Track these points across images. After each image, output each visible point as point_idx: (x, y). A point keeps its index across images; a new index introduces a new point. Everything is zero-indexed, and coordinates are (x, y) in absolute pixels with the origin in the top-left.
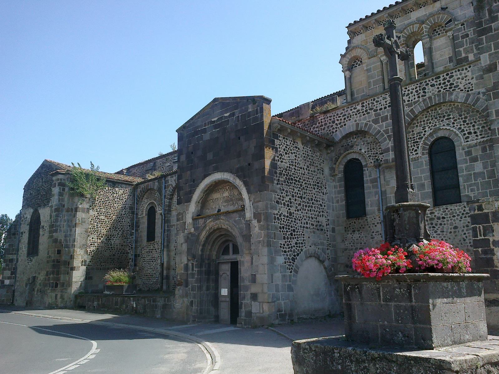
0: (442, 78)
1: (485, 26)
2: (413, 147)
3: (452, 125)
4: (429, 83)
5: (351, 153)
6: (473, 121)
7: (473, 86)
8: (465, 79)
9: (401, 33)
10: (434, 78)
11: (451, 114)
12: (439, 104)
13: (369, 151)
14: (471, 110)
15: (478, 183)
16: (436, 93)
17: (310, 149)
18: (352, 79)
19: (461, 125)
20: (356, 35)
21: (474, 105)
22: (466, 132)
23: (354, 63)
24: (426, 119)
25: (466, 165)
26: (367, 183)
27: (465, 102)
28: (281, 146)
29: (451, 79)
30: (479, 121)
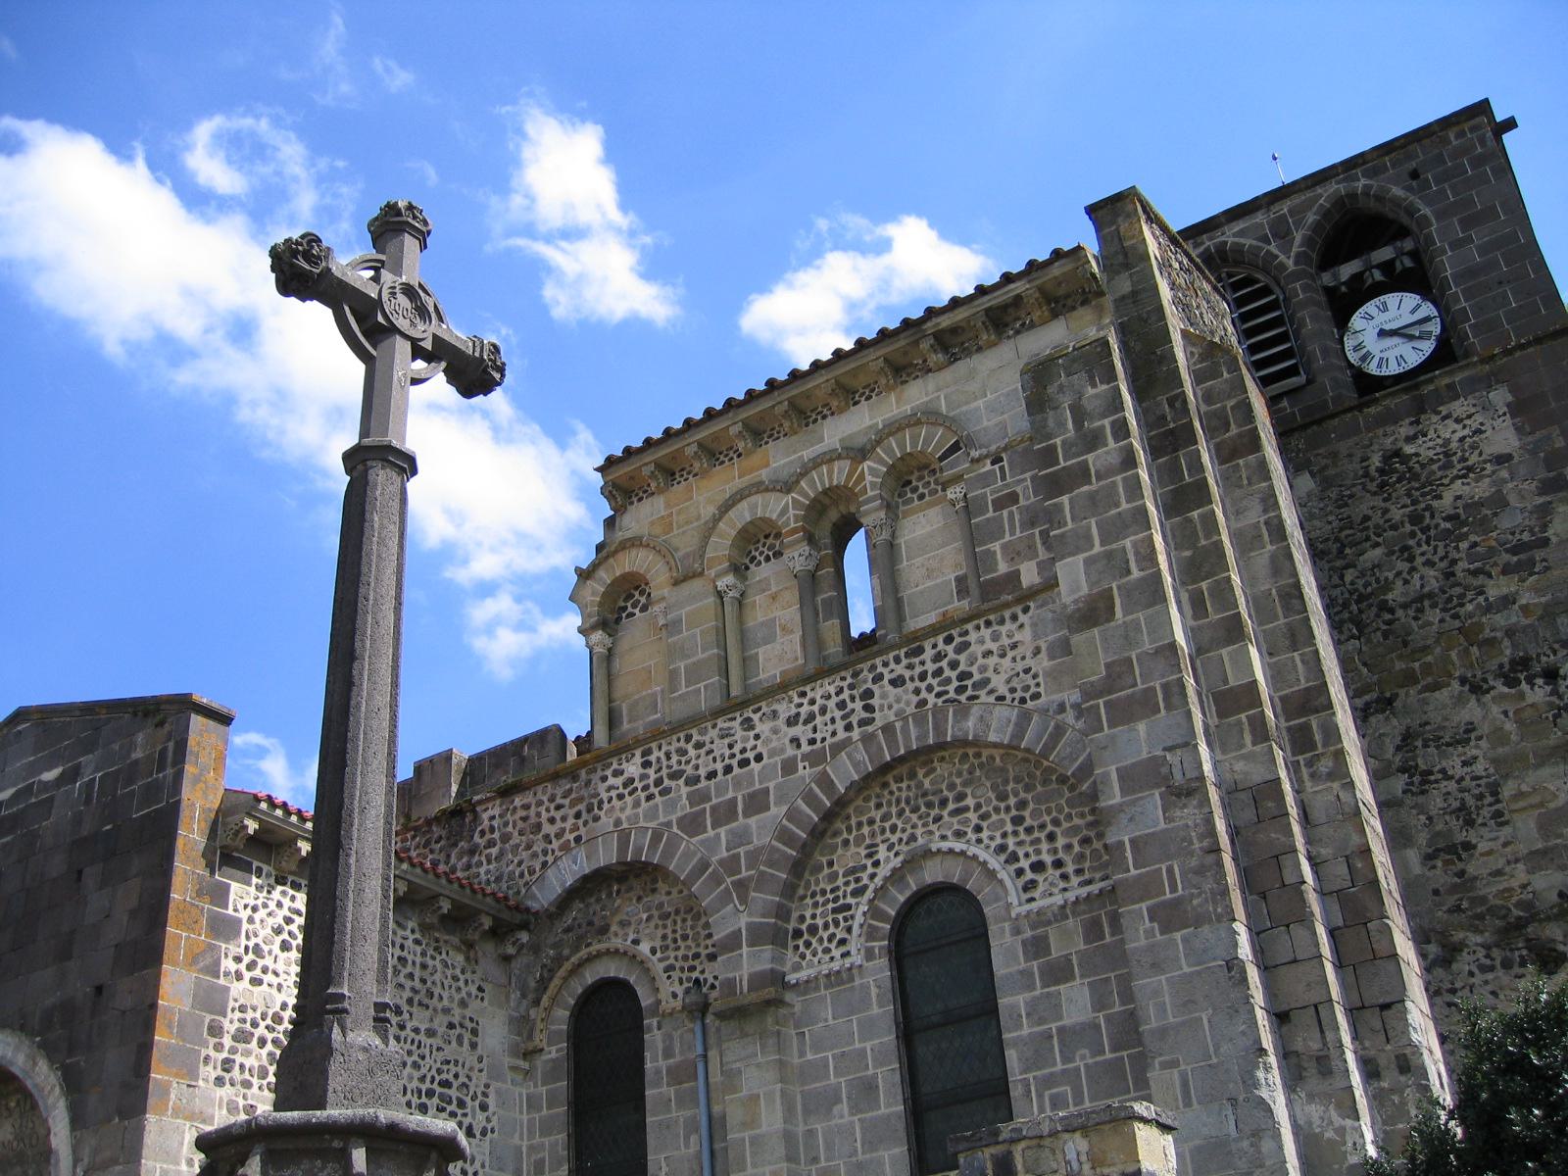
0: (929, 653)
1: (1065, 461)
2: (832, 929)
3: (973, 837)
4: (885, 671)
5: (599, 955)
6: (1047, 819)
7: (1040, 679)
8: (1010, 654)
9: (789, 491)
10: (902, 652)
11: (969, 791)
12: (924, 755)
13: (667, 948)
14: (1038, 773)
15: (1078, 1069)
16: (911, 710)
17: (417, 936)
18: (617, 663)
19: (1004, 835)
20: (635, 499)
21: (1045, 754)
22: (1024, 864)
23: (626, 600)
24: (877, 815)
25: (1028, 995)
26: (658, 1084)
27: (1014, 743)
28: (262, 913)
29: (962, 658)
30: (1069, 817)
